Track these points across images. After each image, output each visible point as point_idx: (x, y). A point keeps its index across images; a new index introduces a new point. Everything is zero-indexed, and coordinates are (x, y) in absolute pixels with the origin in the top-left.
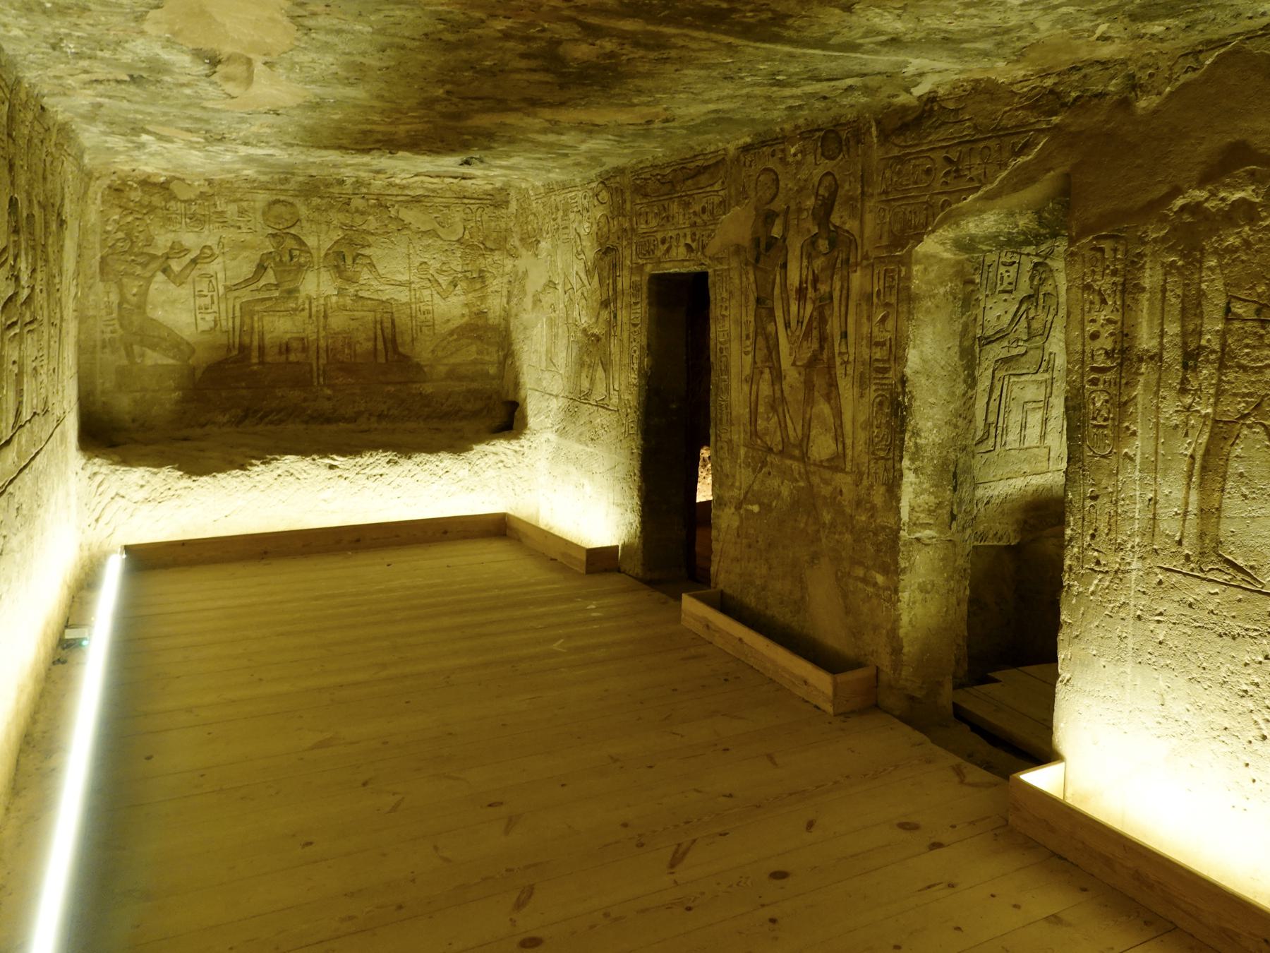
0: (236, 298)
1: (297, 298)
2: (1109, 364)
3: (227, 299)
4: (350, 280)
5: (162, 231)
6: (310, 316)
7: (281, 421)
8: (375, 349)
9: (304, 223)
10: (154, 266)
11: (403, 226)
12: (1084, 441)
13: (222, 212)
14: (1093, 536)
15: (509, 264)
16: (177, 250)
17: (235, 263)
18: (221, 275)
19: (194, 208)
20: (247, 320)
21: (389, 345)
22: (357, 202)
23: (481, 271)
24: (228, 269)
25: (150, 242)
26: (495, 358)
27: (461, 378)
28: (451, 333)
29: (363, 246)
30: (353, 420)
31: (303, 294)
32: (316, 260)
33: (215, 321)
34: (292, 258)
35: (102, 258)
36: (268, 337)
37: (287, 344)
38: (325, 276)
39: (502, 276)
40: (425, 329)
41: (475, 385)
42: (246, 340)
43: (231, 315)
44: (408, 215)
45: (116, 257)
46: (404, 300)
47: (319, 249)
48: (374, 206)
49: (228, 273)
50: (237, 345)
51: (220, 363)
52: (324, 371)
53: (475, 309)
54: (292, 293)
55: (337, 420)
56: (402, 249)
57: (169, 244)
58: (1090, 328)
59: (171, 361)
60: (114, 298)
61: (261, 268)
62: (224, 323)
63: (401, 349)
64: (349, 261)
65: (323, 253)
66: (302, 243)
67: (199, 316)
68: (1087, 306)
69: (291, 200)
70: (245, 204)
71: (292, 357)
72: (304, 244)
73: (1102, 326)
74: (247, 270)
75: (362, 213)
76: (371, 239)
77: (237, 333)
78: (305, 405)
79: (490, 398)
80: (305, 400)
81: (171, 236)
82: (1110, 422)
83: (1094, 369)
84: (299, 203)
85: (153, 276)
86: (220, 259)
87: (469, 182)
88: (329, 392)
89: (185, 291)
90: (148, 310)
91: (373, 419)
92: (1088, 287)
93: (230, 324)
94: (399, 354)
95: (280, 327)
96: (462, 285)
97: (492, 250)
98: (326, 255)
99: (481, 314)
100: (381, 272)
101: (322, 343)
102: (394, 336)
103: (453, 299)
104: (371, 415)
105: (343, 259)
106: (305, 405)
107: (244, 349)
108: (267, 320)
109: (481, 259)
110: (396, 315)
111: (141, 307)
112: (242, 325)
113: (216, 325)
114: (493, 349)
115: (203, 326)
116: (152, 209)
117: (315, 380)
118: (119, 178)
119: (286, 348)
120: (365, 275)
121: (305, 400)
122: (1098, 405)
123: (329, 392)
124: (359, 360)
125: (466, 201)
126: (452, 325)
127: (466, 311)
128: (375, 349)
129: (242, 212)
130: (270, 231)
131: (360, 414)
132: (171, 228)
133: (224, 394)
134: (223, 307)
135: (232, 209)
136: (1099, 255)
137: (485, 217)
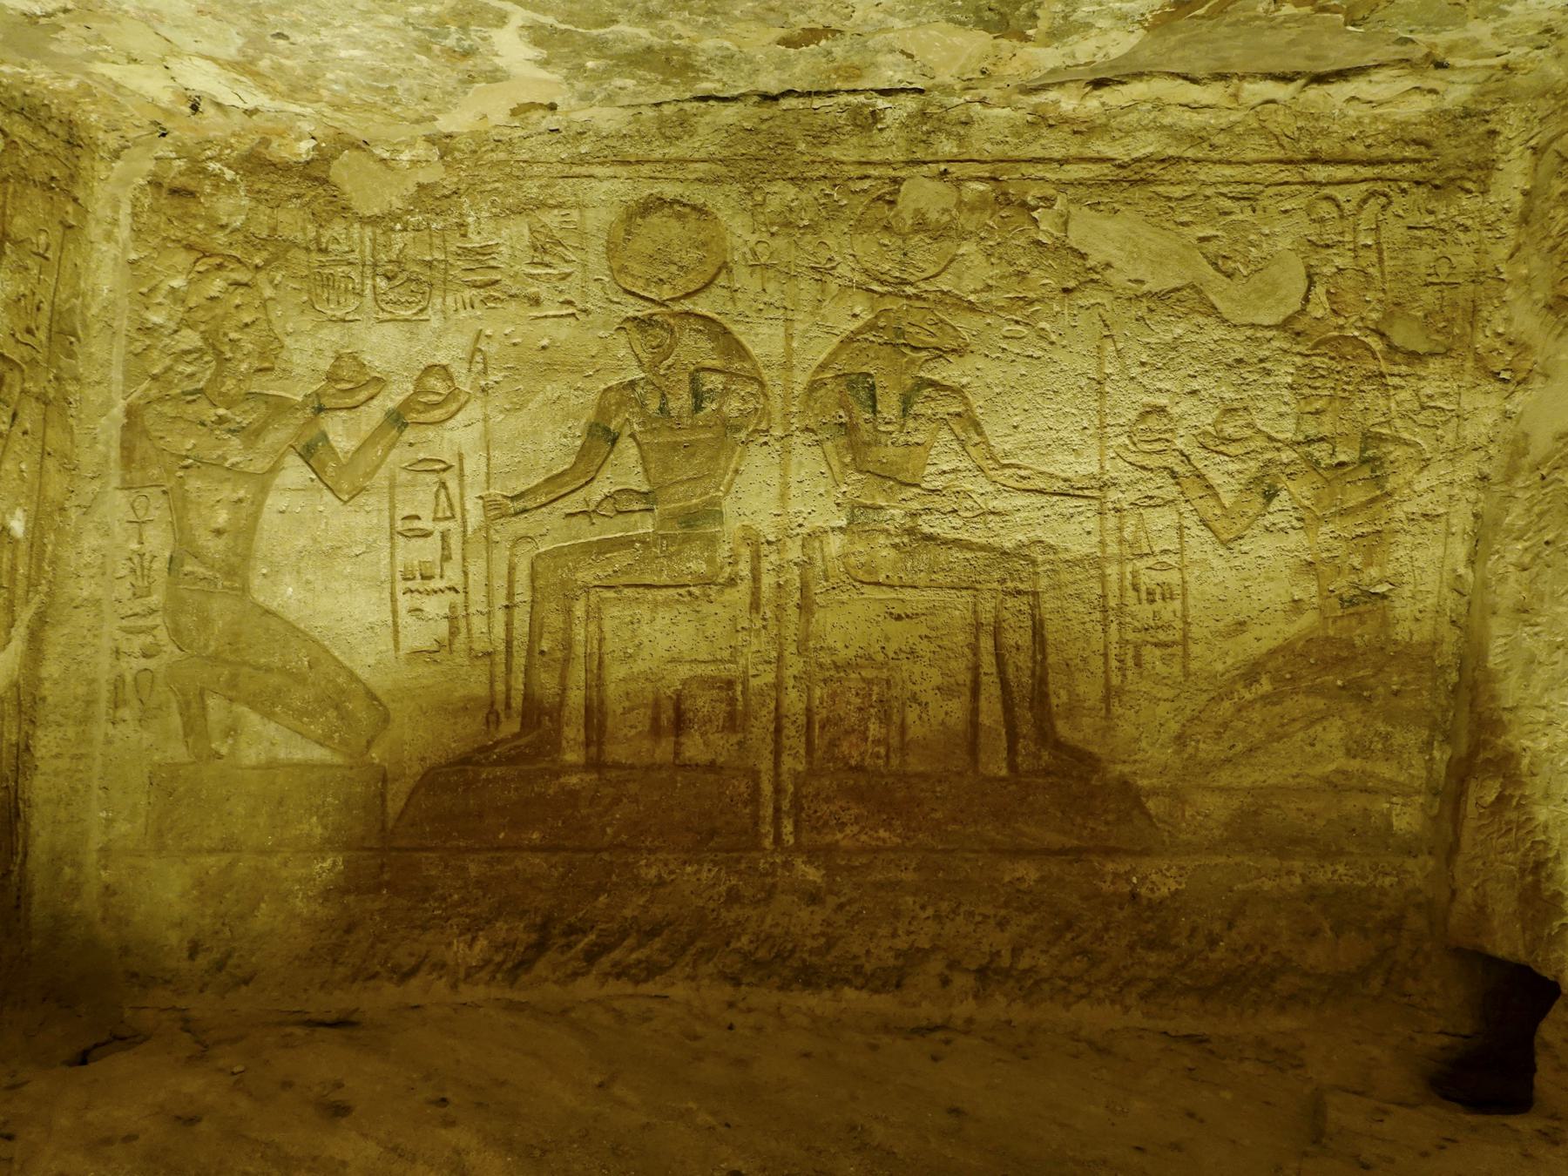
0: (519, 540)
1: (712, 541)
3: (490, 543)
4: (892, 478)
5: (307, 323)
6: (755, 606)
7: (652, 970)
8: (974, 724)
9: (743, 278)
10: (279, 435)
11: (1086, 275)
13: (485, 251)
15: (1484, 409)
16: (349, 382)
17: (517, 422)
18: (474, 465)
19: (399, 240)
20: (555, 621)
21: (1025, 715)
22: (923, 195)
23: (1370, 438)
24: (501, 440)
25: (269, 359)
26: (1416, 770)
27: (1285, 844)
28: (1251, 674)
29: (940, 353)
30: (893, 980)
31: (732, 526)
32: (776, 405)
33: (452, 619)
34: (698, 398)
35: (130, 412)
36: (616, 672)
37: (678, 701)
38: (808, 461)
39: (1454, 454)
40: (1151, 655)
41: (1335, 873)
42: (547, 681)
43: (501, 600)
44: (1104, 235)
45: (168, 409)
46: (1080, 547)
47: (787, 366)
48: (980, 204)
49: (499, 457)
50: (517, 702)
51: (465, 760)
52: (797, 805)
53: (1341, 584)
54: (695, 521)
55: (836, 982)
56: (1076, 361)
57: (325, 365)
59: (319, 754)
60: (158, 541)
61: (602, 436)
62: (479, 624)
63: (1063, 729)
64: (889, 406)
65: (801, 379)
66: (733, 348)
67: (404, 602)
69: (699, 195)
70: (551, 218)
71: (694, 748)
72: (741, 352)
74: (555, 445)
75: (939, 233)
76: (966, 324)
77: (519, 660)
78: (730, 916)
79: (1395, 924)
80: (733, 897)
81: (332, 336)
84: (724, 203)
85: (274, 470)
86: (474, 411)
87: (1340, 91)
88: (813, 874)
89: (362, 520)
90: (256, 582)
91: (961, 981)
93: (499, 631)
94: (1058, 745)
95: (657, 641)
96: (1297, 491)
97: (1414, 357)
98: (813, 387)
99: (1363, 602)
100: (1001, 444)
101: (794, 701)
102: (1041, 681)
103: (1261, 546)
104: (953, 965)
105: (862, 408)
106: (730, 916)
107: (539, 714)
108: (614, 615)
109: (1371, 394)
110: (1048, 604)
111: (236, 571)
112: (535, 634)
113: (454, 632)
114: (1408, 738)
115: (417, 636)
116: (277, 248)
117: (766, 828)
118: (182, 151)
119: (674, 717)
120: (944, 459)
121: (733, 897)
123: (814, 875)
124: (915, 764)
125: (1320, 173)
126: (1254, 644)
127: (1307, 590)
128: (974, 724)
129: (543, 248)
130: (633, 309)
131: (914, 957)
132: (332, 310)
133: (474, 870)
134: (477, 569)
135: (512, 237)
137: (1395, 232)
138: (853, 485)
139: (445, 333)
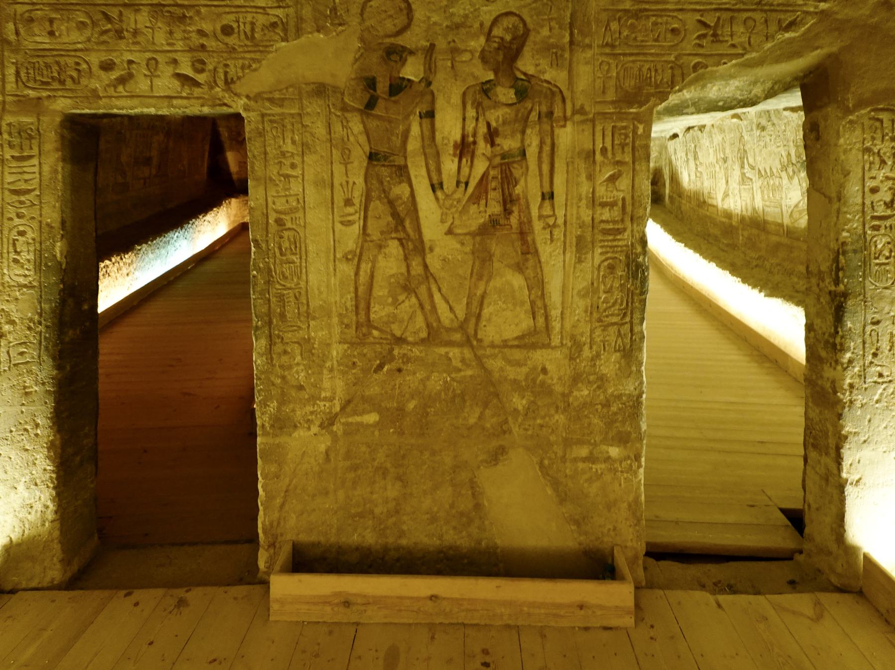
2: (889, 212)
12: (864, 277)
14: (875, 355)
58: (870, 184)
68: (867, 166)
73: (882, 182)
82: (892, 259)
83: (874, 218)
92: (868, 150)
122: (879, 246)
136: (878, 124)
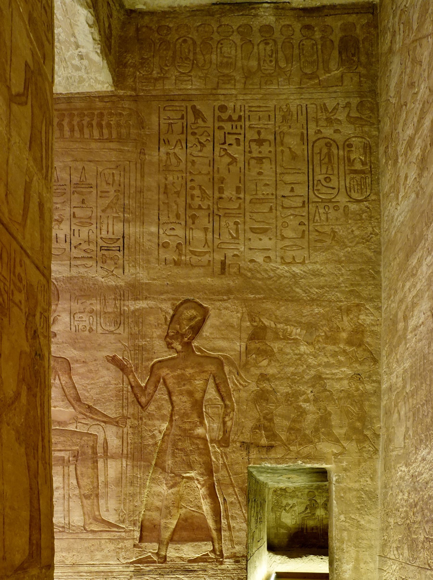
10: (283, 508)
16: (288, 504)
24: (299, 509)
31: (317, 514)
36: (308, 526)
54: (314, 514)
60: (274, 516)
61: (306, 508)
66: (316, 501)
71: (314, 531)
74: (303, 509)
89: (289, 515)
95: (311, 523)
107: (302, 529)
111: (280, 519)
115: (293, 523)
119: (312, 529)
129: (302, 495)
135: (300, 494)
138: (325, 511)
139: (295, 501)
